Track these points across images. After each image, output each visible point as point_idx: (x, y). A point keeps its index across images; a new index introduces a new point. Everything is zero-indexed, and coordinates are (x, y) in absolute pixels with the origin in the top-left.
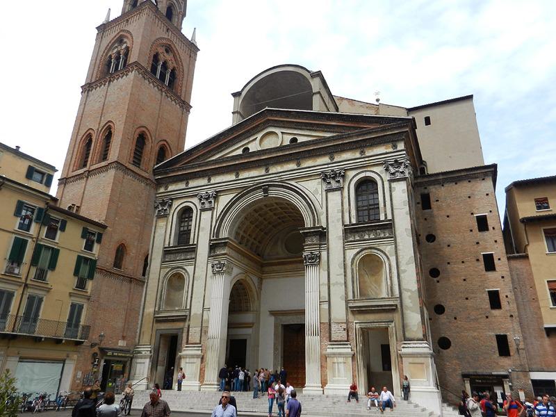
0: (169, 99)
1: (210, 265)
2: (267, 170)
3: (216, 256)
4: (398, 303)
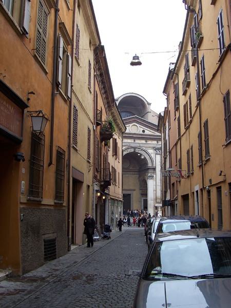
2: (134, 141)
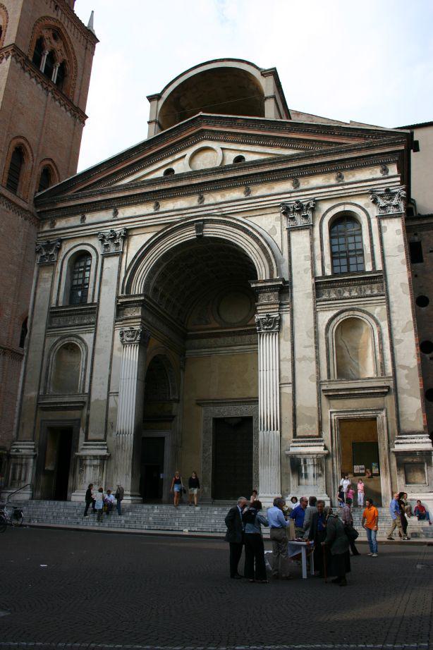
0: (57, 103)
1: (117, 333)
3: (127, 319)
4: (391, 384)
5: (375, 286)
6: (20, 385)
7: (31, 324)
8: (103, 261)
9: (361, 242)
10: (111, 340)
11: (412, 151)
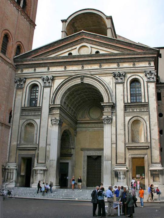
1: (50, 120)
2: (83, 67)
5: (145, 108)
6: (9, 139)
7: (14, 114)
8: (43, 89)
9: (141, 91)
10: (47, 122)
11: (159, 57)
